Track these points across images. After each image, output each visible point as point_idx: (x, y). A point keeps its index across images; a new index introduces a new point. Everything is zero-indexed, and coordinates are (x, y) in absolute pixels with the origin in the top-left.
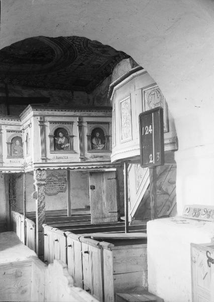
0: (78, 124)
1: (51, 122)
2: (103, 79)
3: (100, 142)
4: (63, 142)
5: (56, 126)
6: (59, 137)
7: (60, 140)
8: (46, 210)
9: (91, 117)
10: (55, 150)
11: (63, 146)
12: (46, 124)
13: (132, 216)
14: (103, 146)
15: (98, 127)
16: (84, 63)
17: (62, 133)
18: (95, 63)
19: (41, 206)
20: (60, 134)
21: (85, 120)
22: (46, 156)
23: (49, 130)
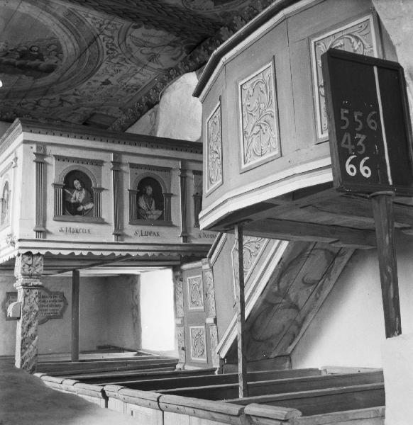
0: (112, 165)
1: (58, 158)
2: (142, 113)
3: (153, 206)
4: (81, 200)
5: (68, 167)
6: (73, 188)
10: (64, 214)
11: (81, 208)
12: (47, 160)
13: (223, 356)
14: (160, 213)
16: (111, 79)
17: (81, 182)
18: (132, 81)
19: (30, 334)
20: (76, 182)
22: (44, 226)
23: (54, 174)
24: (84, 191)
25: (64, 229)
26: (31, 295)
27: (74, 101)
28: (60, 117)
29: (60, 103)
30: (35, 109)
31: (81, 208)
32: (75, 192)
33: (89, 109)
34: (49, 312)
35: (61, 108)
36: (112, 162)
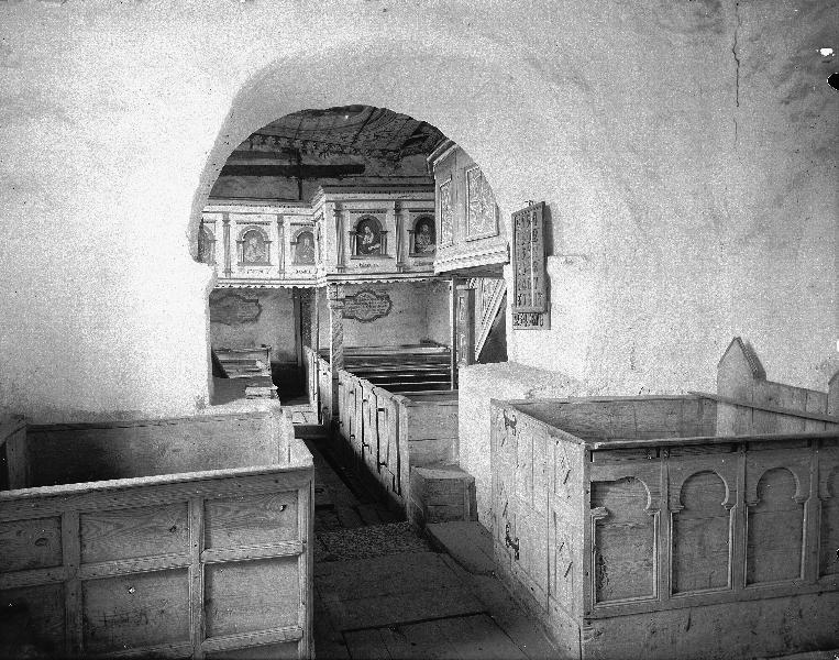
8: (346, 345)
9: (413, 203)
12: (343, 213)
21: (405, 205)
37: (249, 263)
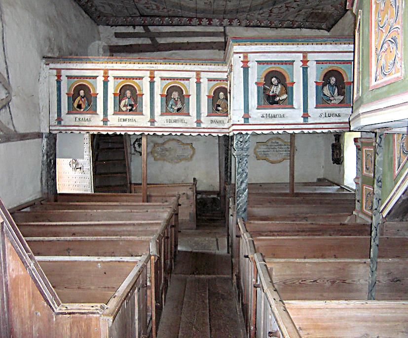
7: (274, 88)
9: (324, 52)
11: (278, 98)
14: (342, 98)
15: (334, 68)
17: (277, 78)
24: (280, 86)
25: (265, 116)
26: (243, 162)
27: (296, 6)
28: (289, 18)
29: (286, 9)
30: (270, 16)
31: (278, 98)
32: (273, 87)
33: (310, 10)
34: (284, 155)
35: (287, 12)
36: (301, 61)
37: (171, 114)
